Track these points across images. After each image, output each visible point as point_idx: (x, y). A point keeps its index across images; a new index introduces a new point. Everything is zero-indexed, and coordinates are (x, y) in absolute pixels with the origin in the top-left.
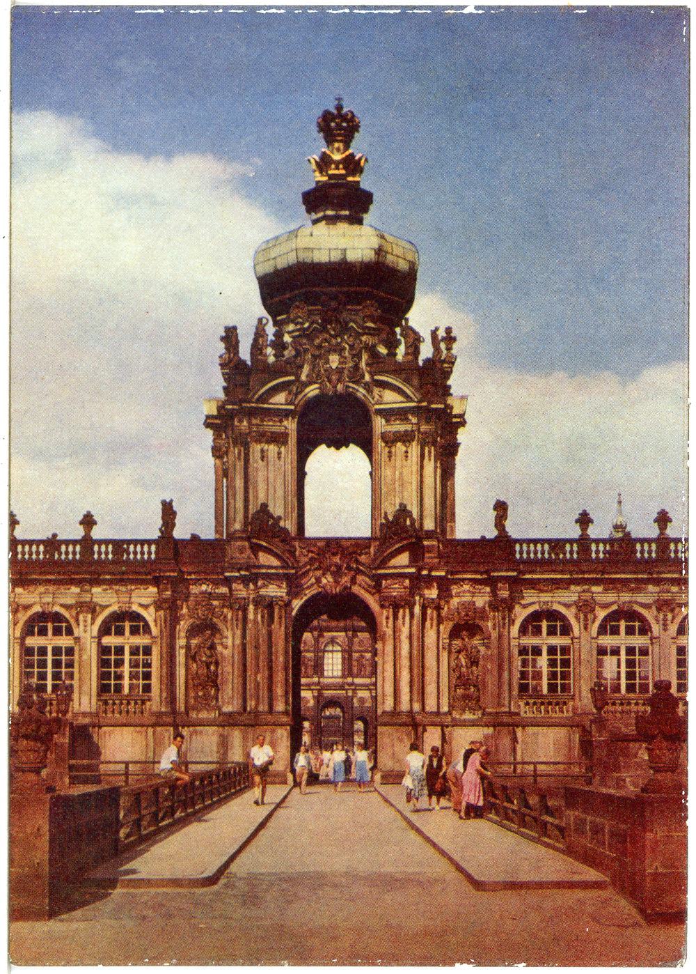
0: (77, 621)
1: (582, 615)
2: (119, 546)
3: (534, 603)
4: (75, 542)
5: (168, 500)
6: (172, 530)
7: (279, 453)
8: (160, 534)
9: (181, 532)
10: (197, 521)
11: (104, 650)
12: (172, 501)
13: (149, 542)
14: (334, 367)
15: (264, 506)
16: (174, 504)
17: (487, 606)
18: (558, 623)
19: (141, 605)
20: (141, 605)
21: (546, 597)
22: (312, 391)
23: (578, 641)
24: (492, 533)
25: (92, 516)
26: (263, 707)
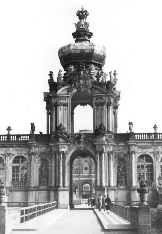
0: (5, 159)
1: (156, 156)
2: (18, 136)
3: (141, 152)
4: (5, 136)
5: (33, 123)
6: (34, 132)
7: (65, 109)
8: (30, 133)
9: (37, 132)
10: (42, 128)
11: (14, 168)
12: (34, 123)
13: (27, 135)
14: (81, 84)
15: (61, 125)
16: (34, 124)
17: (127, 153)
18: (148, 158)
19: (24, 154)
21: (145, 150)
22: (75, 91)
24: (129, 132)
25: (10, 128)
26: (61, 185)
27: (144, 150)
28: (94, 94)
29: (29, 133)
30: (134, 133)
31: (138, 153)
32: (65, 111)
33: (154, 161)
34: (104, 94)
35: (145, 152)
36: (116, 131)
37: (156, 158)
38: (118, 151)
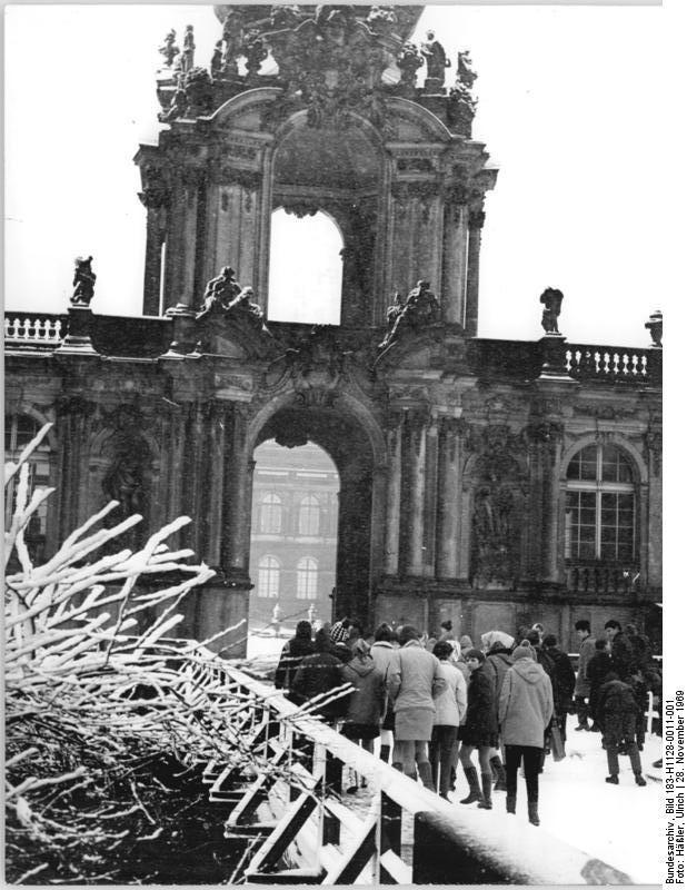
7: (249, 200)
13: (53, 318)
17: (525, 433)
19: (36, 405)
20: (36, 405)
21: (605, 426)
23: (646, 488)
27: (600, 422)
28: (389, 139)
29: (61, 305)
30: (569, 341)
31: (575, 437)
32: (244, 209)
33: (644, 479)
34: (436, 145)
35: (608, 433)
36: (473, 327)
37: (652, 462)
38: (484, 423)
